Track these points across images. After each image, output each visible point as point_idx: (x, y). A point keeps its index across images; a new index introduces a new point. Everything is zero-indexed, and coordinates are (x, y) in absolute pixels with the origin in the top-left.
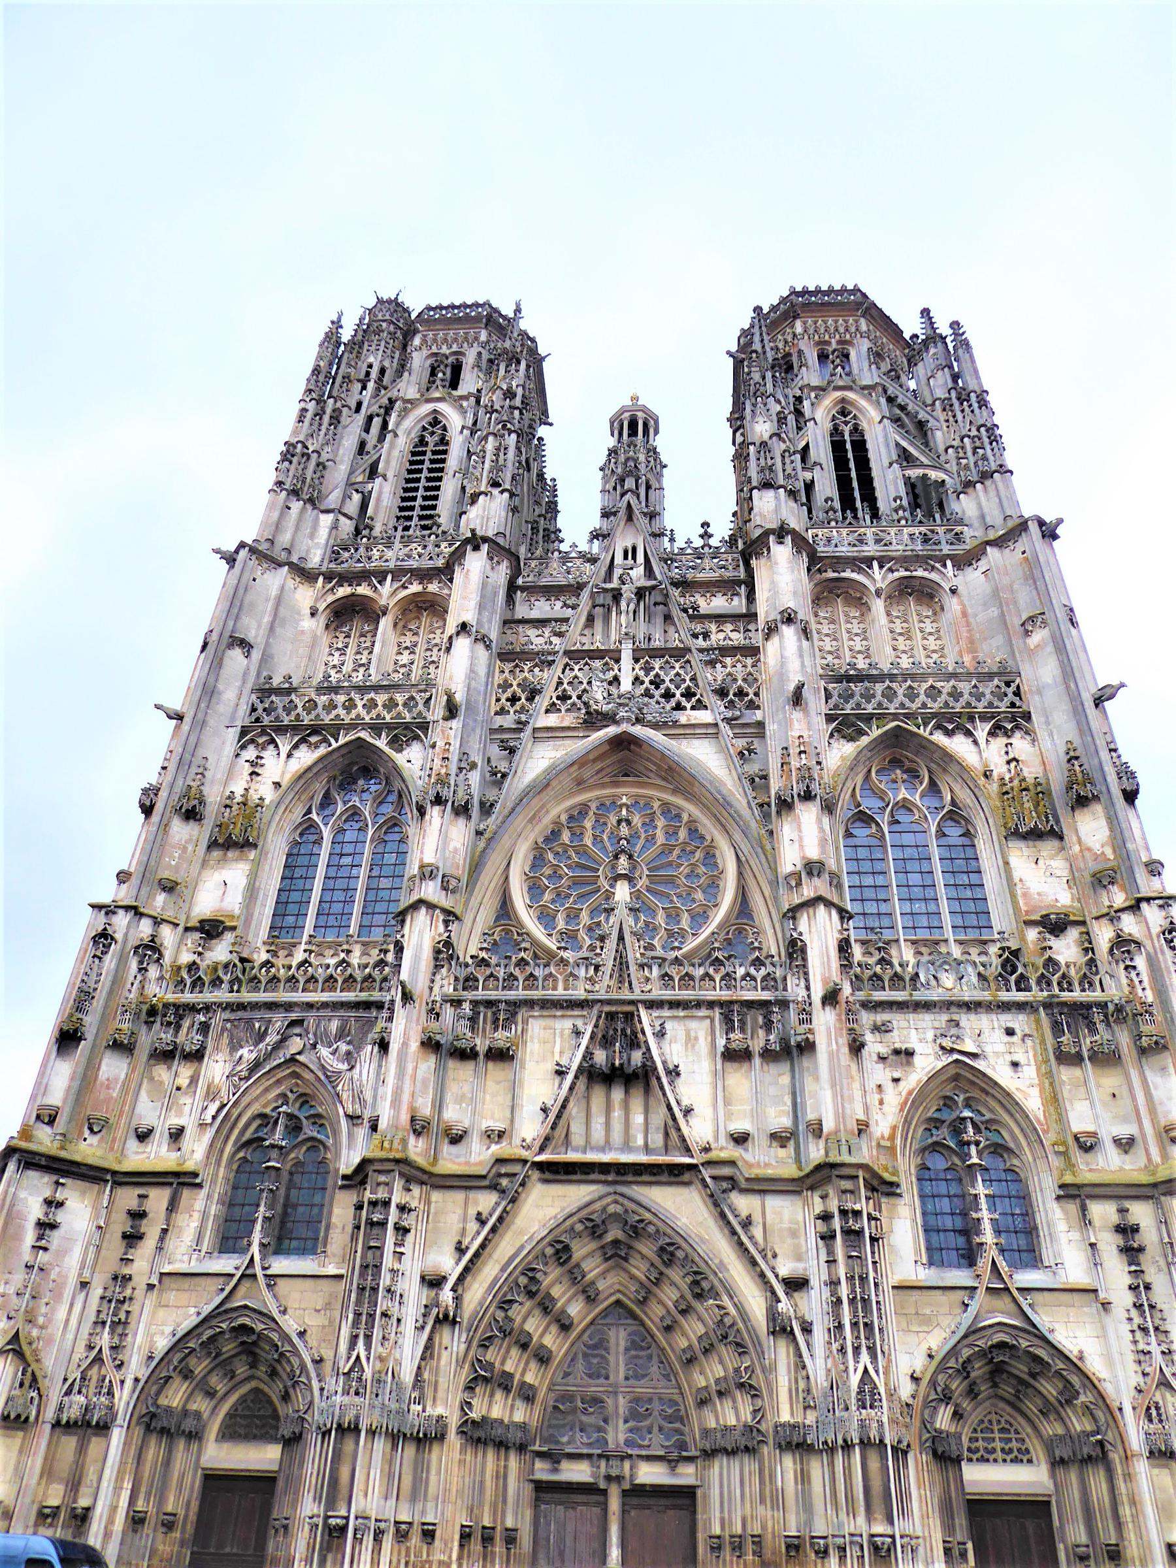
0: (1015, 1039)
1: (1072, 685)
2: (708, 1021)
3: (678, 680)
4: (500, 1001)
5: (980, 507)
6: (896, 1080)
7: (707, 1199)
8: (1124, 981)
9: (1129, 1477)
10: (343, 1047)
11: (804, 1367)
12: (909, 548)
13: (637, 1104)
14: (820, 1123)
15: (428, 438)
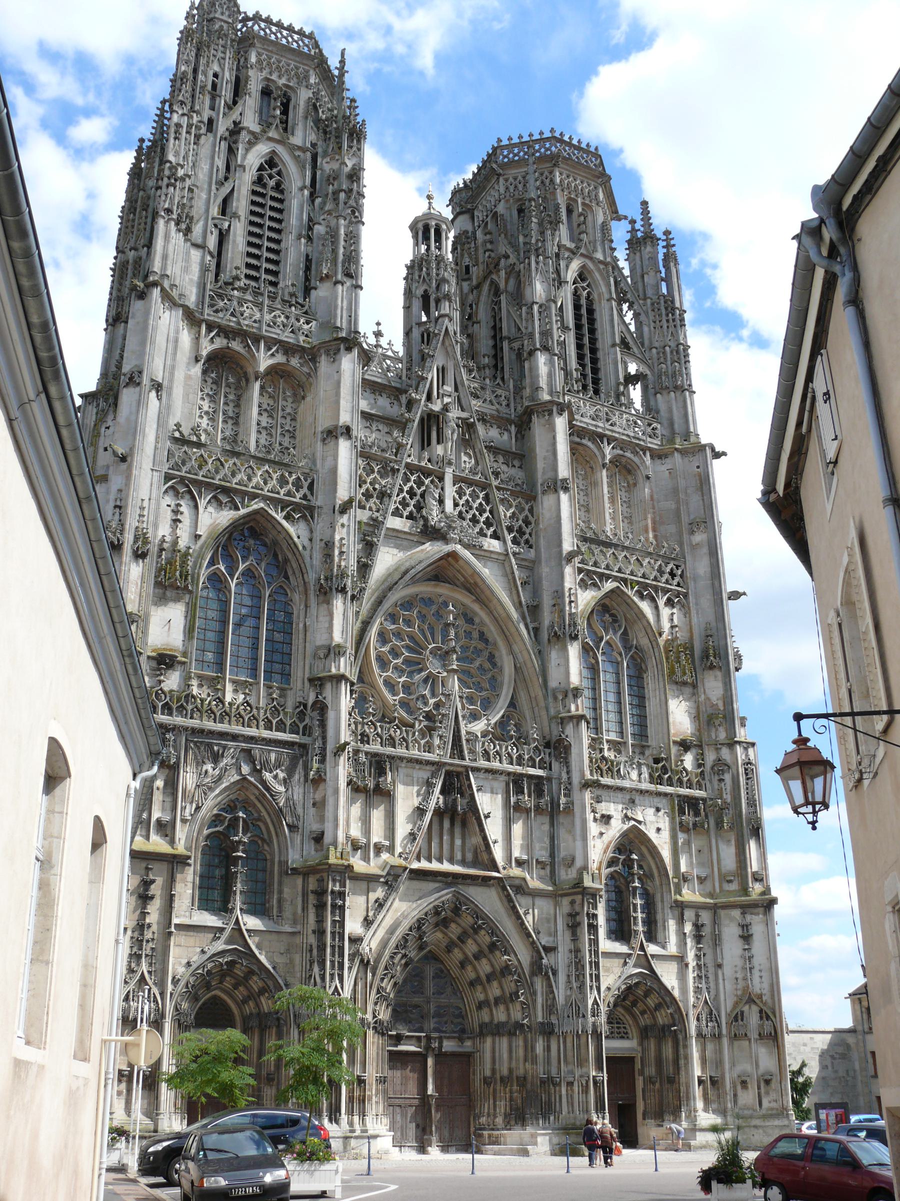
1: (716, 583)
2: (504, 784)
3: (481, 510)
4: (384, 755)
5: (670, 411)
6: (601, 834)
7: (504, 898)
8: (716, 787)
9: (686, 1046)
10: (282, 775)
11: (553, 992)
12: (626, 432)
13: (458, 831)
14: (573, 860)
15: (266, 179)
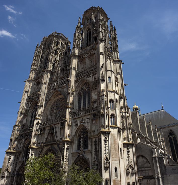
0: (89, 119)
6: (76, 128)
